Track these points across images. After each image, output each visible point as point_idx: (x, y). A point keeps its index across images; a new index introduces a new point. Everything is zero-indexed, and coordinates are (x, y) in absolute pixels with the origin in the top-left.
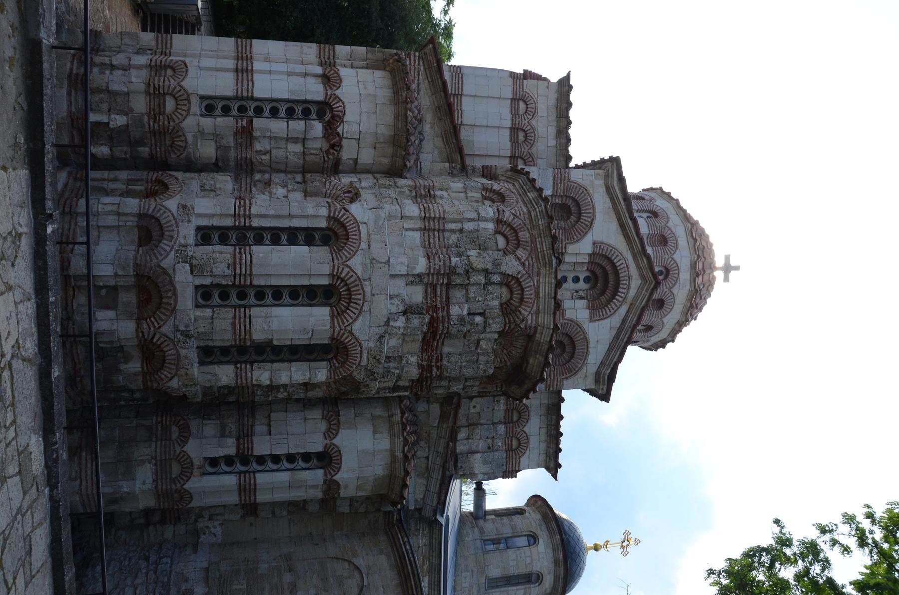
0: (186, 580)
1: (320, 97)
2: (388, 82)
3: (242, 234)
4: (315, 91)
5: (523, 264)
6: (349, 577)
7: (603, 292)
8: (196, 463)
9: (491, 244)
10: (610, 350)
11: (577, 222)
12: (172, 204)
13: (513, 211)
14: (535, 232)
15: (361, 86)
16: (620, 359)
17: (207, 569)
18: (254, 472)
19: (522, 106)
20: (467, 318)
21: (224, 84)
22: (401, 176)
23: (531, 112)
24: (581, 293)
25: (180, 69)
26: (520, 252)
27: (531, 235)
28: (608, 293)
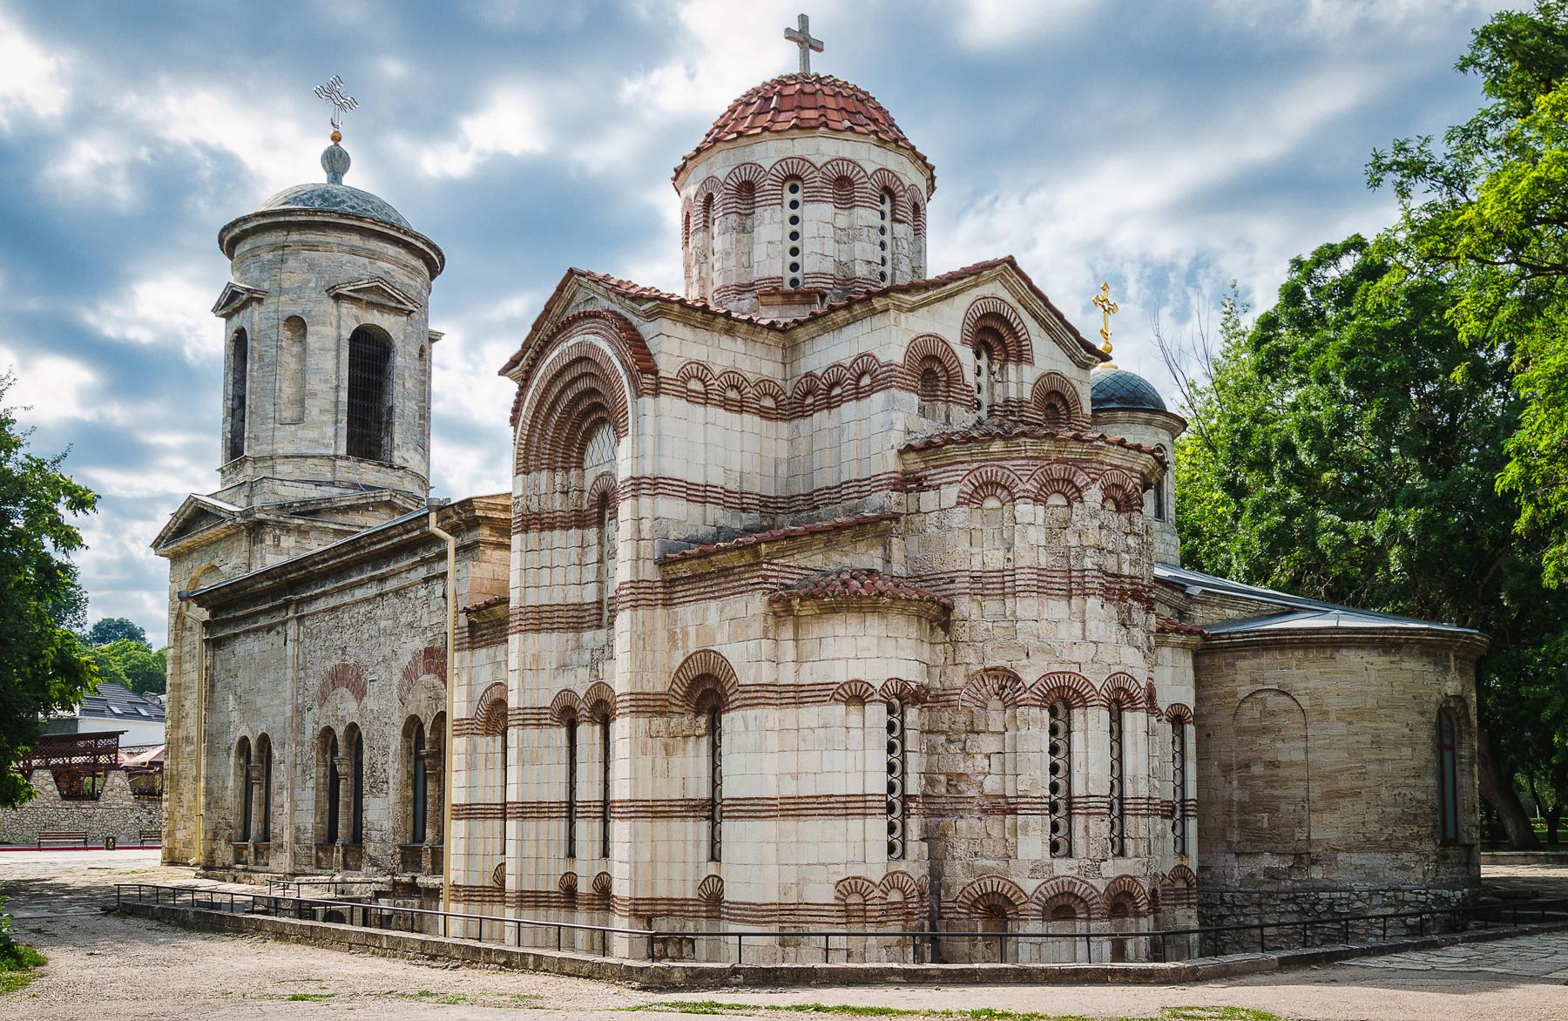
0: (1252, 875)
1: (884, 708)
2: (854, 620)
3: (1061, 805)
4: (877, 714)
5: (1094, 480)
6: (1265, 706)
7: (1000, 338)
8: (1178, 862)
9: (1061, 513)
10: (1059, 342)
11: (940, 362)
12: (1029, 886)
13: (1025, 479)
14: (1053, 457)
15: (865, 654)
16: (1075, 333)
17: (1238, 855)
18: (1183, 800)
19: (694, 385)
20: (1134, 556)
21: (877, 827)
22: (947, 609)
23: (701, 371)
24: (996, 368)
25: (850, 886)
26: (1080, 479)
27: (1057, 461)
28: (1003, 331)
